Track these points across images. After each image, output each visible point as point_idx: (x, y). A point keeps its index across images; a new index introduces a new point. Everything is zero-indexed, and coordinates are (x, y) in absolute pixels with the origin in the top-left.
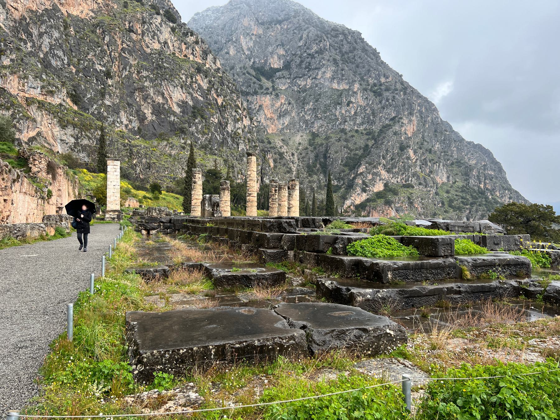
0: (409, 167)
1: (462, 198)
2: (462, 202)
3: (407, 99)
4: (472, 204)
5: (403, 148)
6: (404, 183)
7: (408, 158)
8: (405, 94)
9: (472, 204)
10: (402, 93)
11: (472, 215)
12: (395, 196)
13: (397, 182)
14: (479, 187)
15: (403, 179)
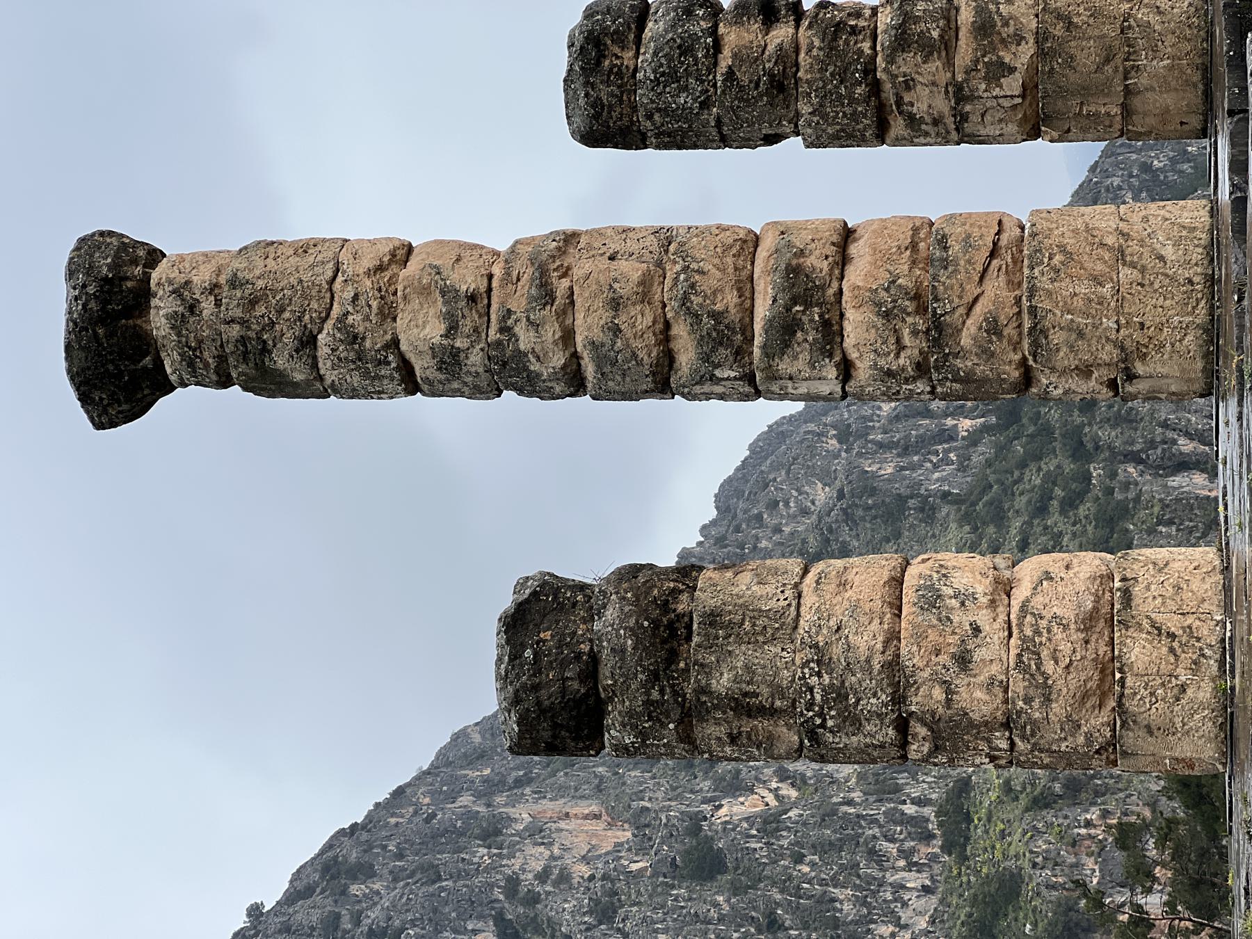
0: (828, 815)
1: (1041, 510)
2: (1070, 504)
3: (400, 856)
4: (1081, 451)
5: (704, 861)
6: (935, 847)
7: (770, 823)
8: (365, 871)
9: (1081, 451)
10: (356, 889)
11: (1152, 444)
12: (1028, 890)
13: (926, 890)
14: (974, 438)
15: (906, 854)
